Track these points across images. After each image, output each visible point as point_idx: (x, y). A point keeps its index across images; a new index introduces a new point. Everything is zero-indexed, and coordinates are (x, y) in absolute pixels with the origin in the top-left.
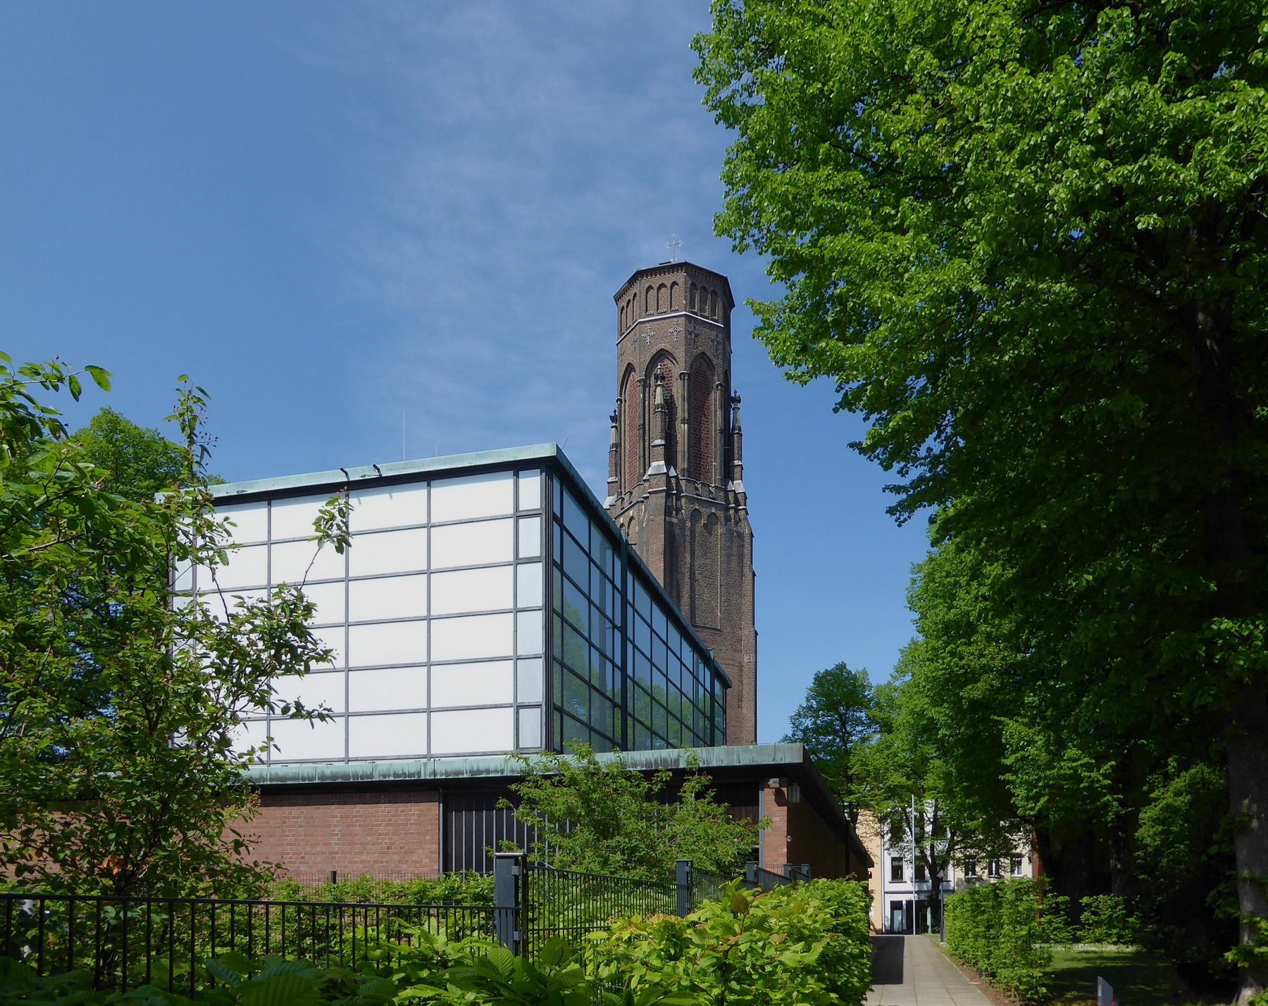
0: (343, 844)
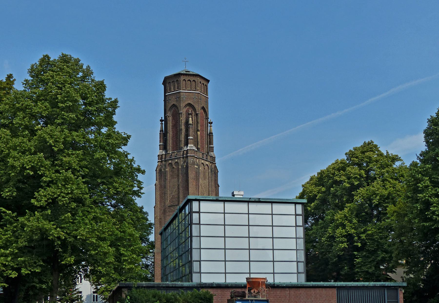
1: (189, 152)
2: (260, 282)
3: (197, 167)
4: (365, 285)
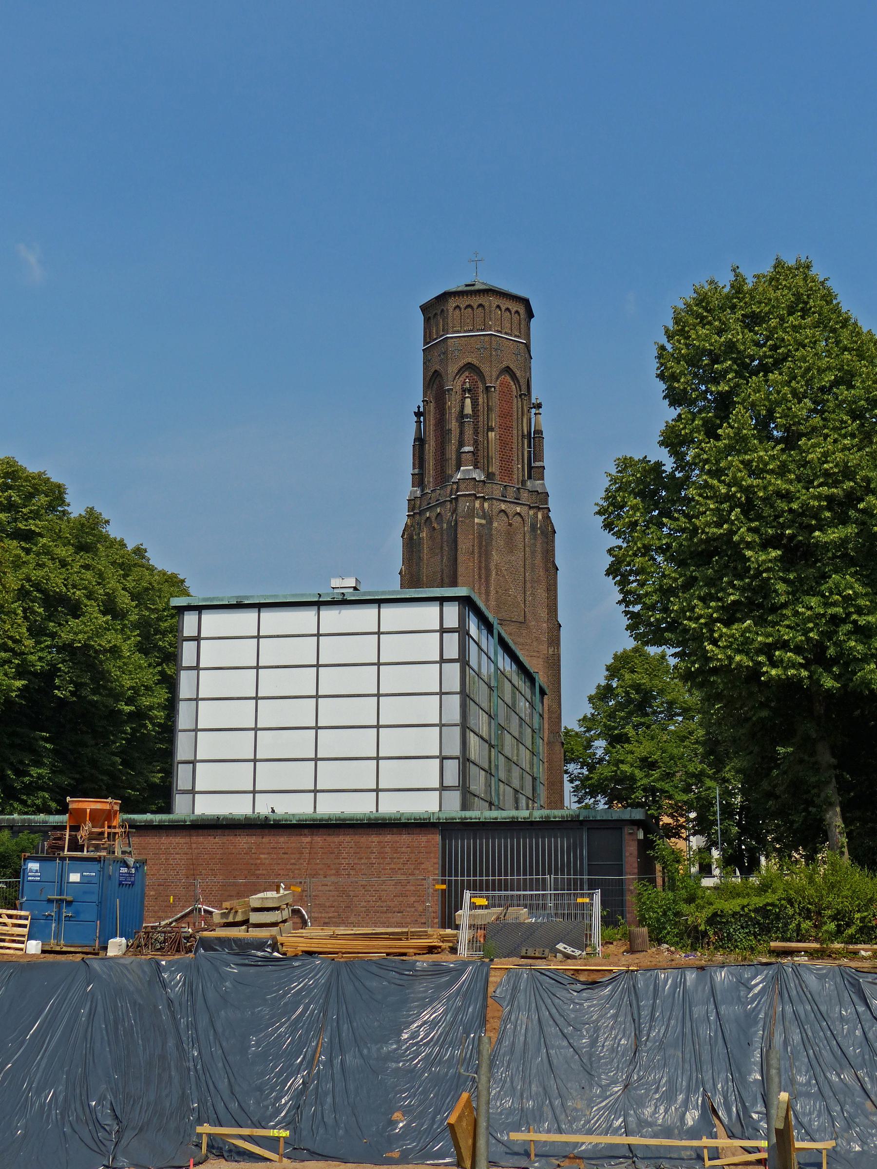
0: (379, 858)
1: (462, 486)
2: (88, 811)
3: (483, 522)
4: (517, 818)
